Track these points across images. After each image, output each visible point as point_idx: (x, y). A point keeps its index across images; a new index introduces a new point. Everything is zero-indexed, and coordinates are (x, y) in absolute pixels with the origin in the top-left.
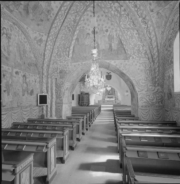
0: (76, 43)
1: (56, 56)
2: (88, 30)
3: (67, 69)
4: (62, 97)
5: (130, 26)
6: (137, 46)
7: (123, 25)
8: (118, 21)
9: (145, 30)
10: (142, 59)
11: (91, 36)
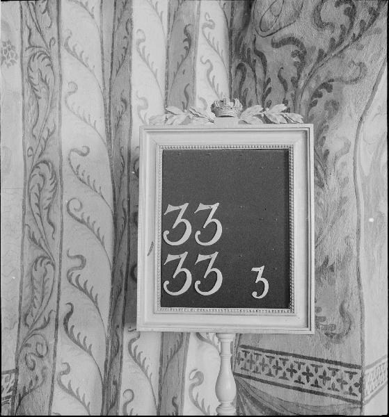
4: (343, 263)
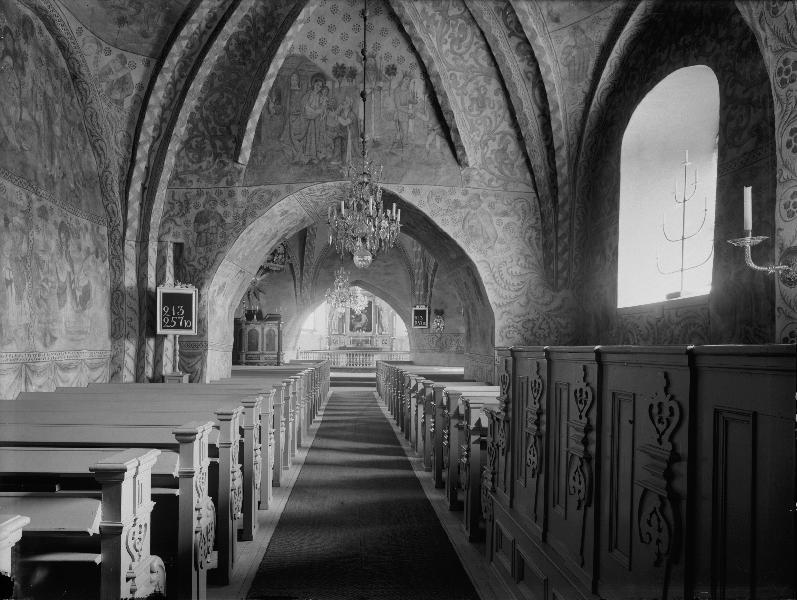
0: (272, 105)
1: (183, 154)
2: (318, 62)
3: (229, 208)
5: (476, 61)
6: (498, 137)
8: (434, 40)
9: (526, 81)
10: (511, 187)
11: (329, 84)
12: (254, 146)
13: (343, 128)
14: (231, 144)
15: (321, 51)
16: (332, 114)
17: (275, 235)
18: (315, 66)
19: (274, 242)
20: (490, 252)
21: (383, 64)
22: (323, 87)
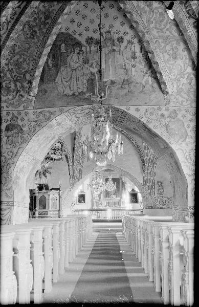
2: (77, 36)
3: (25, 122)
5: (171, 32)
7: (155, 30)
12: (40, 85)
13: (93, 74)
14: (26, 85)
15: (78, 30)
16: (86, 66)
17: (54, 138)
18: (75, 38)
19: (53, 141)
20: (183, 144)
21: (116, 36)
22: (80, 50)
